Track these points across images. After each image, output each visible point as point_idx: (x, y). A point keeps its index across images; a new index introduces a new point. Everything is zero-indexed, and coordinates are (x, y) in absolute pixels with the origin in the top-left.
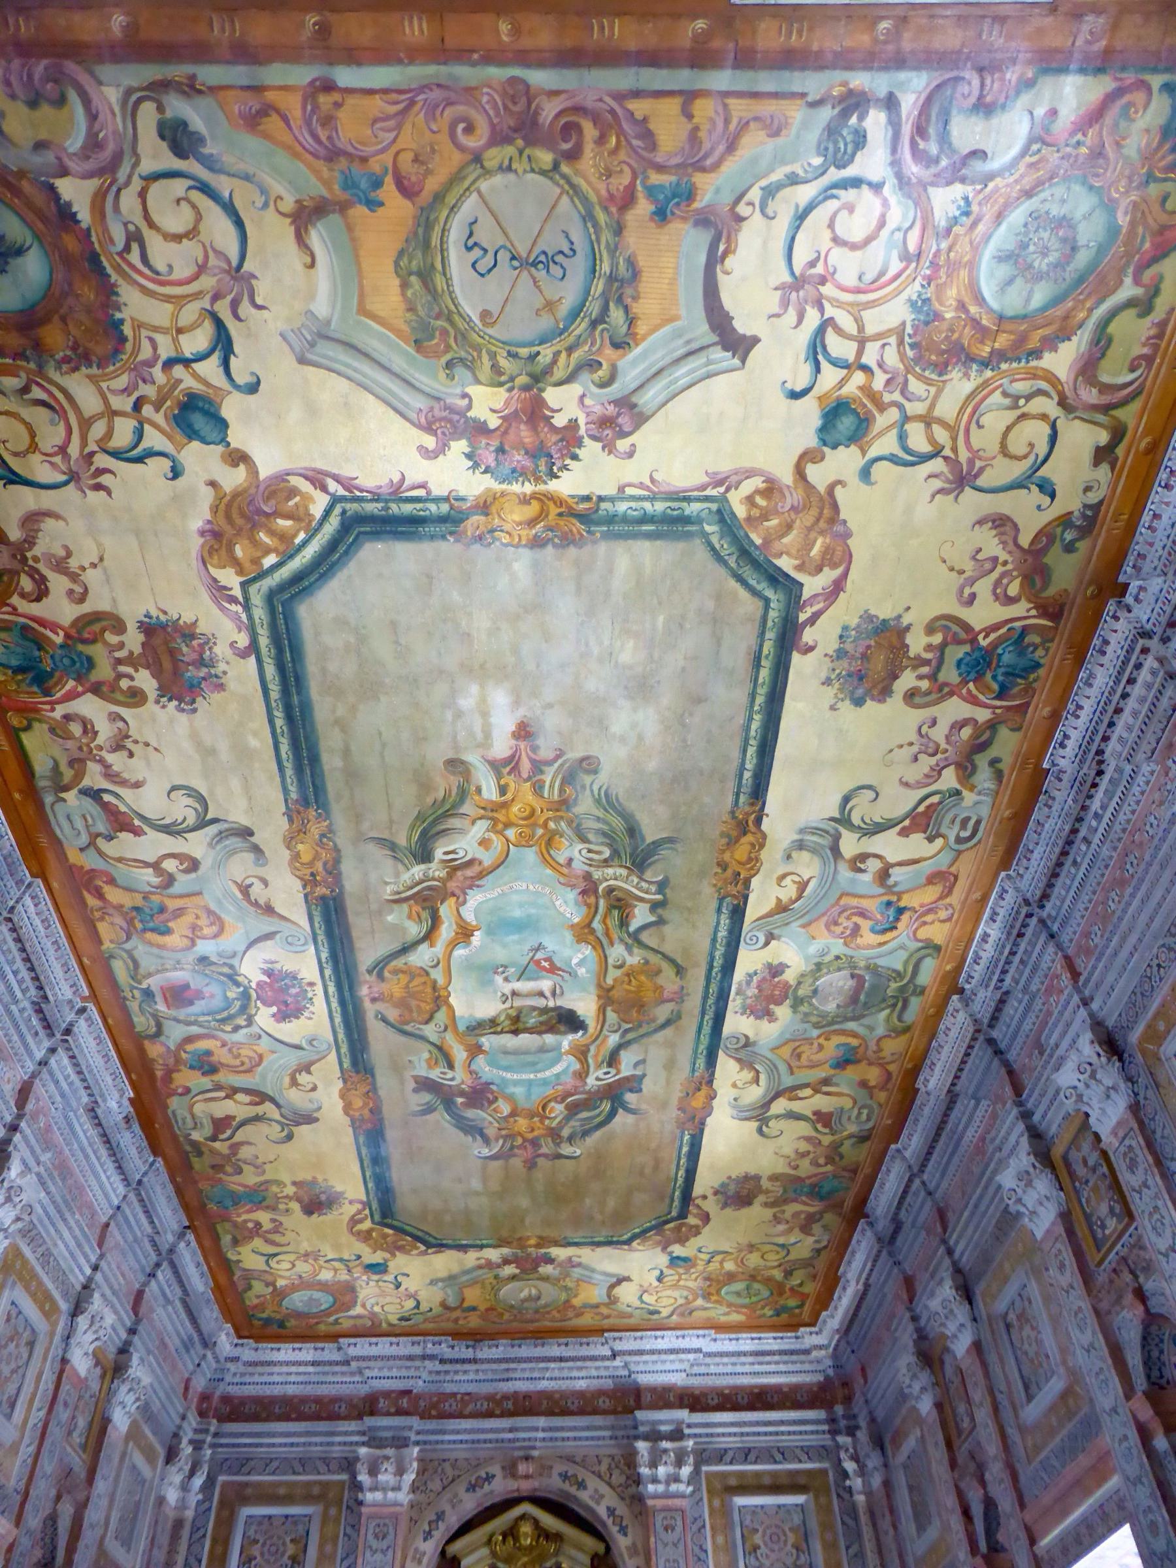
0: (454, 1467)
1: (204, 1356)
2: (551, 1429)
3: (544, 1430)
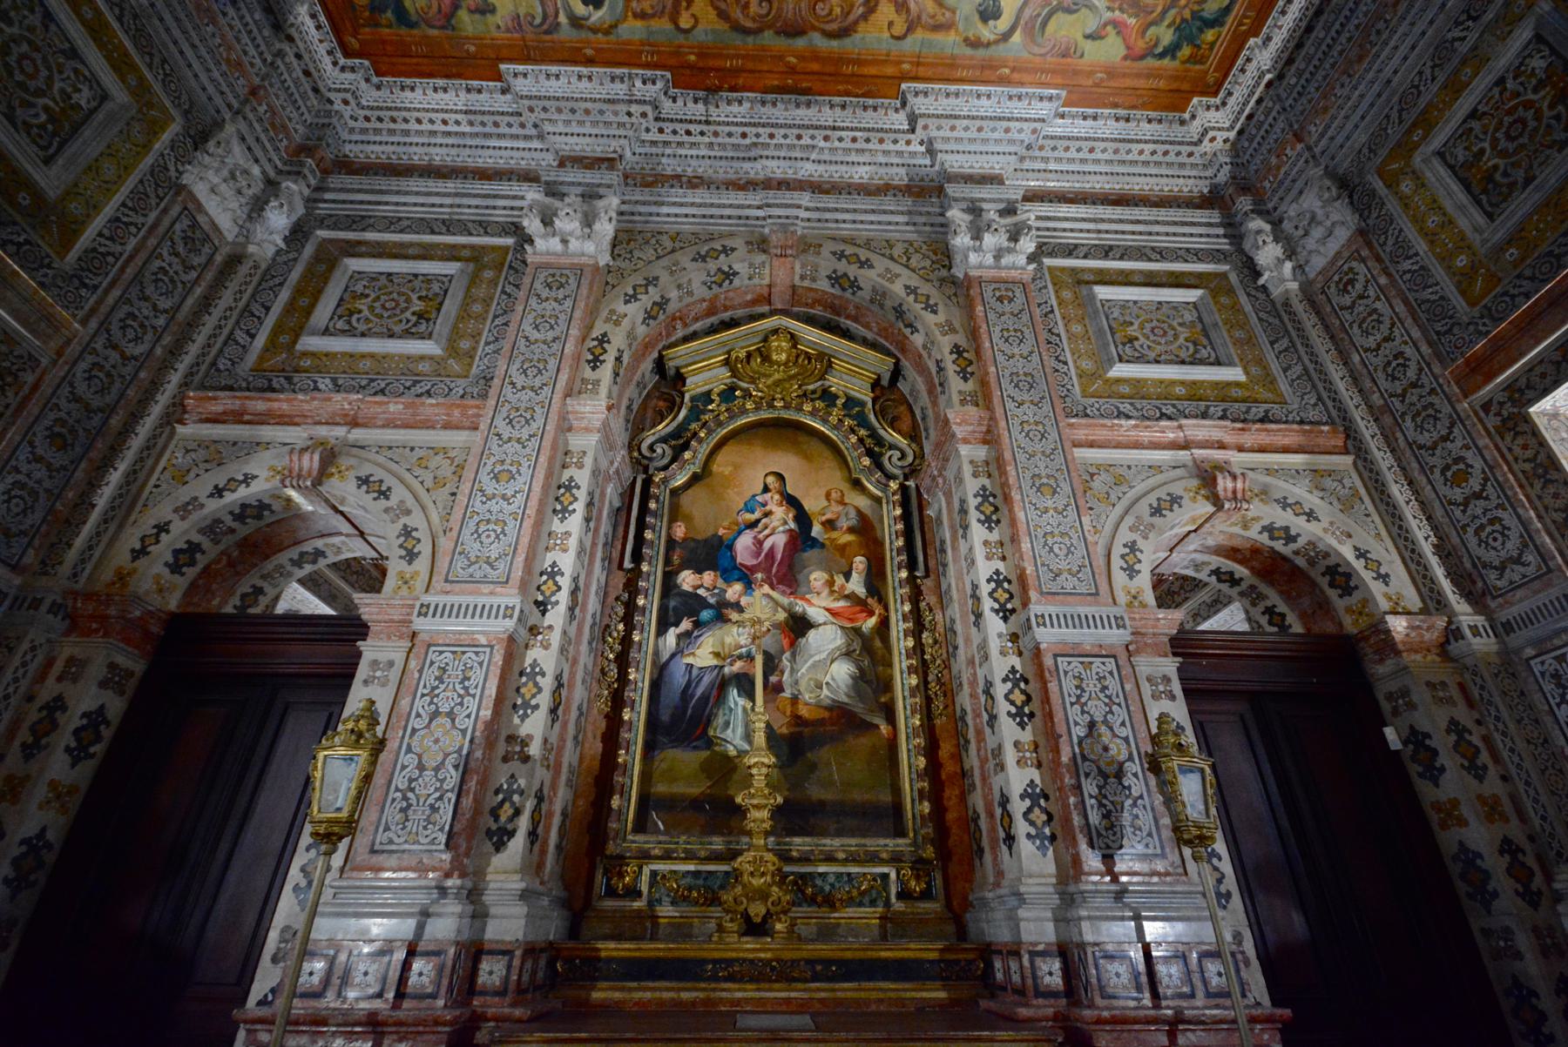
0: (673, 239)
1: (280, 54)
2: (818, 209)
3: (807, 209)
